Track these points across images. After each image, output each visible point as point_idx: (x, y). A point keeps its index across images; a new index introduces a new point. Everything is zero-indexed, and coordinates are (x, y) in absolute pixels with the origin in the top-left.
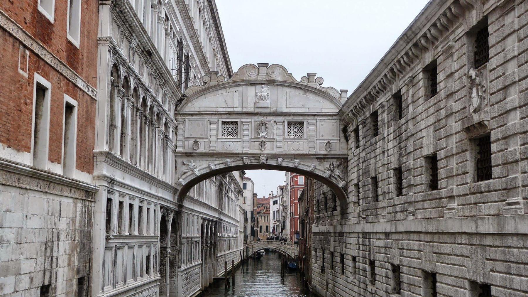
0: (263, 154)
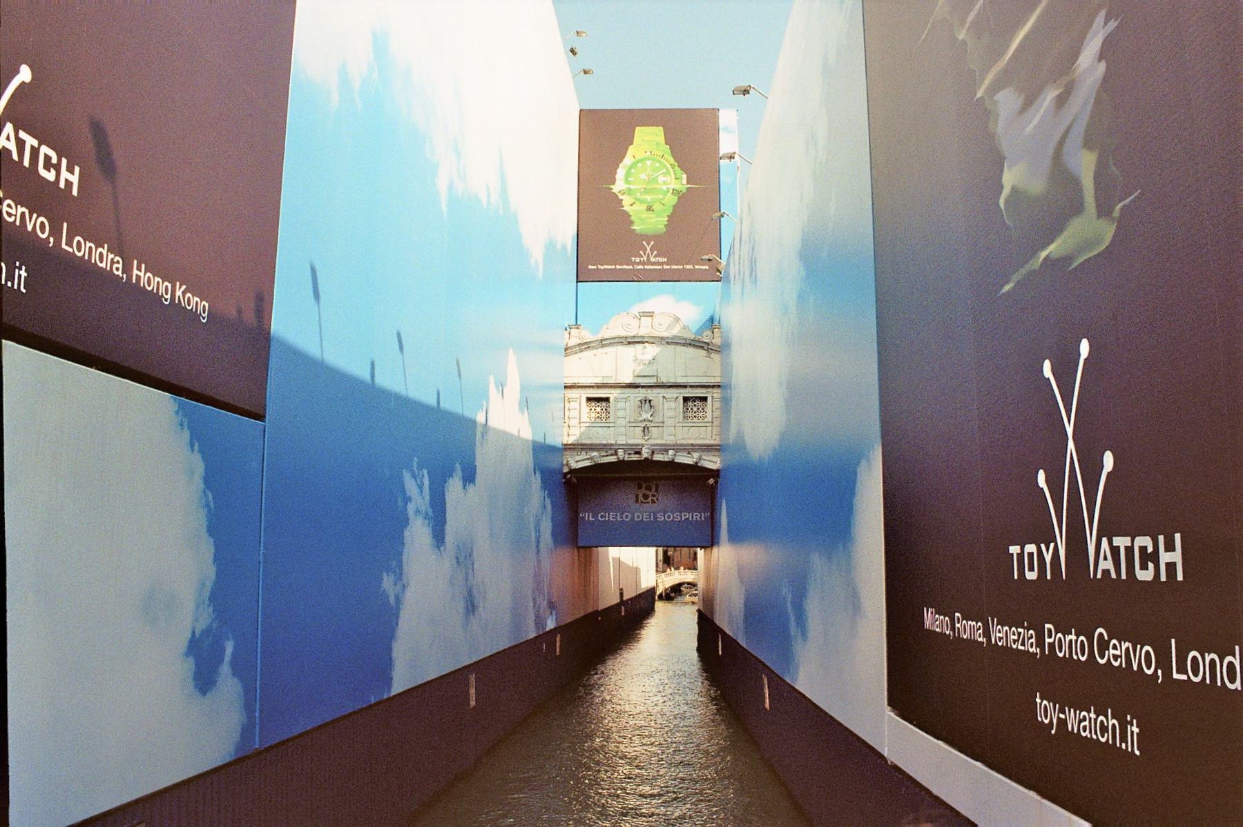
0: (647, 445)
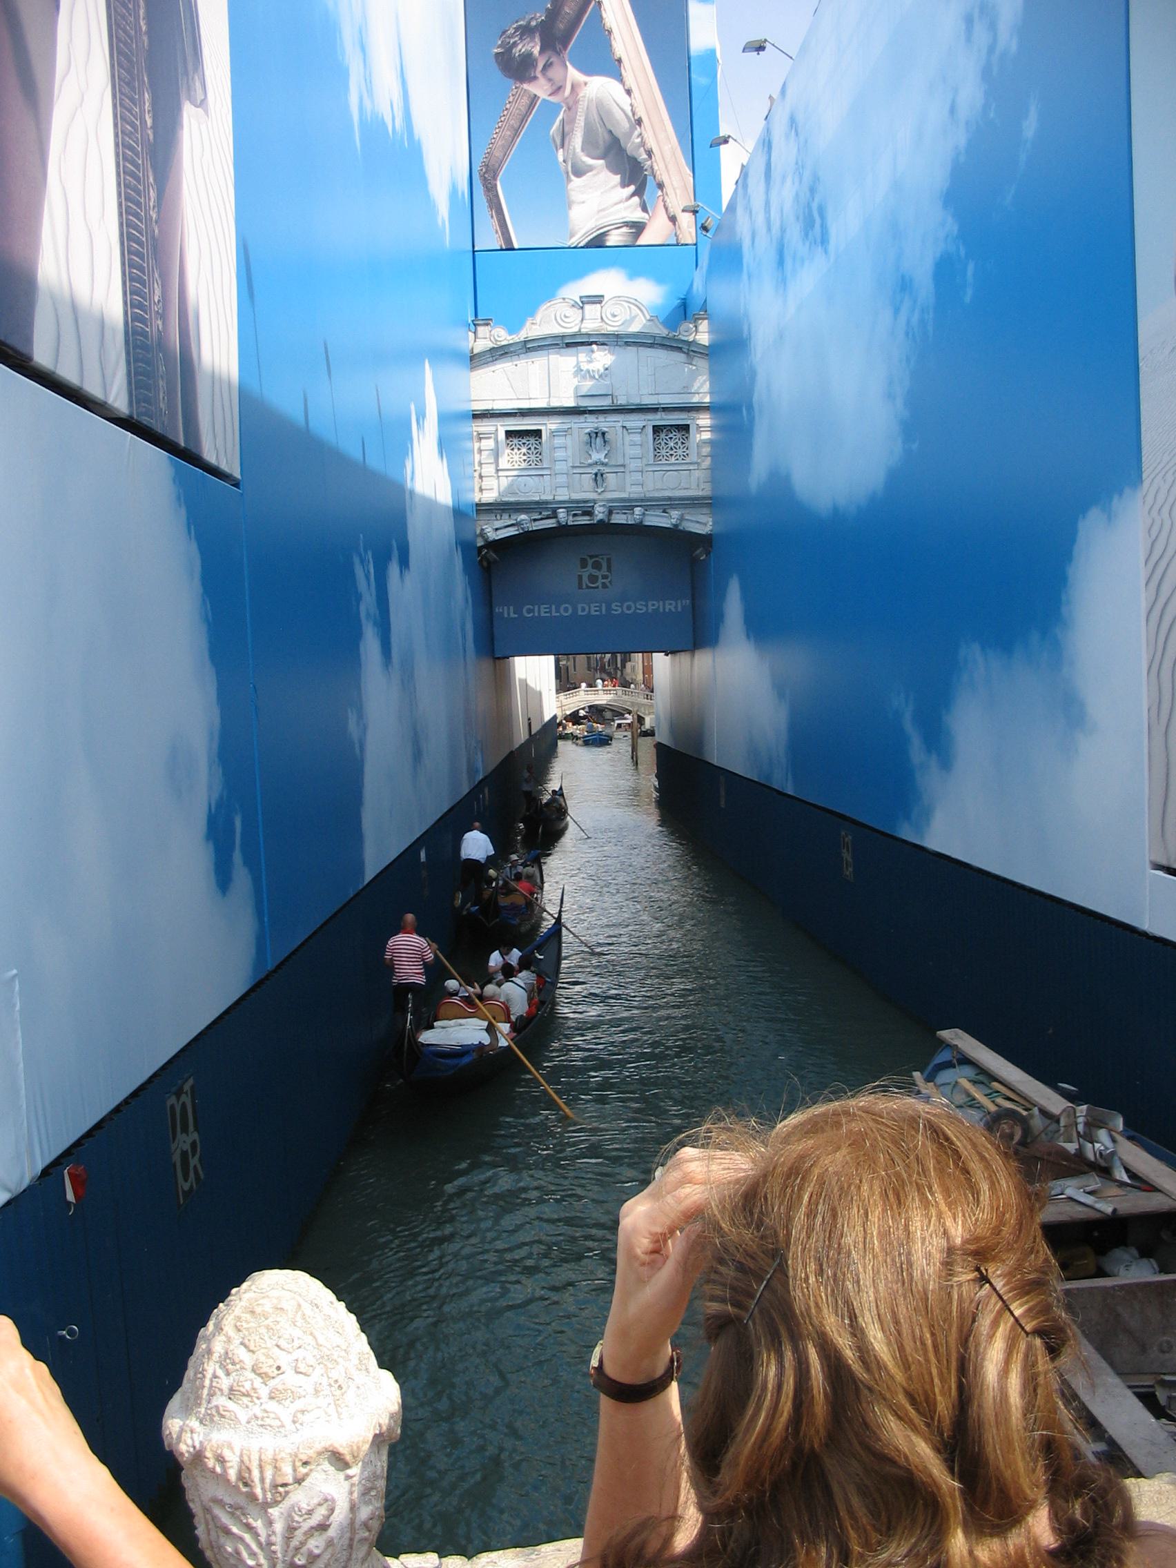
0: (602, 501)
